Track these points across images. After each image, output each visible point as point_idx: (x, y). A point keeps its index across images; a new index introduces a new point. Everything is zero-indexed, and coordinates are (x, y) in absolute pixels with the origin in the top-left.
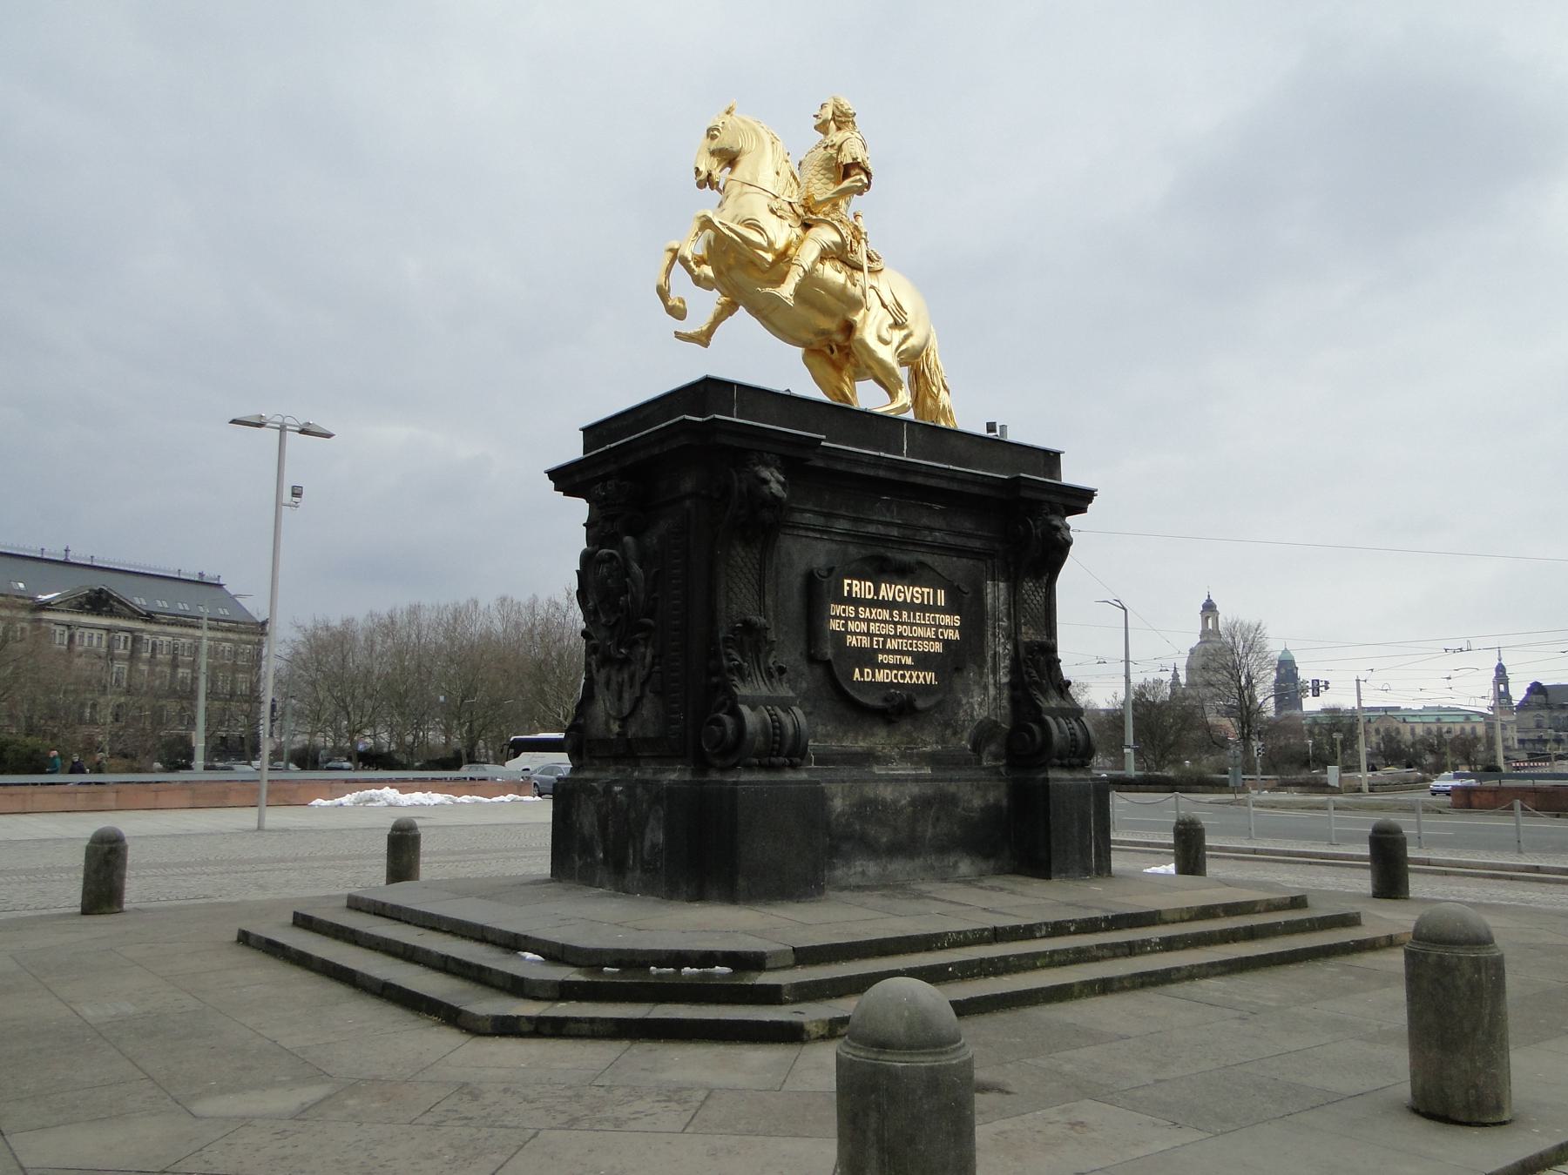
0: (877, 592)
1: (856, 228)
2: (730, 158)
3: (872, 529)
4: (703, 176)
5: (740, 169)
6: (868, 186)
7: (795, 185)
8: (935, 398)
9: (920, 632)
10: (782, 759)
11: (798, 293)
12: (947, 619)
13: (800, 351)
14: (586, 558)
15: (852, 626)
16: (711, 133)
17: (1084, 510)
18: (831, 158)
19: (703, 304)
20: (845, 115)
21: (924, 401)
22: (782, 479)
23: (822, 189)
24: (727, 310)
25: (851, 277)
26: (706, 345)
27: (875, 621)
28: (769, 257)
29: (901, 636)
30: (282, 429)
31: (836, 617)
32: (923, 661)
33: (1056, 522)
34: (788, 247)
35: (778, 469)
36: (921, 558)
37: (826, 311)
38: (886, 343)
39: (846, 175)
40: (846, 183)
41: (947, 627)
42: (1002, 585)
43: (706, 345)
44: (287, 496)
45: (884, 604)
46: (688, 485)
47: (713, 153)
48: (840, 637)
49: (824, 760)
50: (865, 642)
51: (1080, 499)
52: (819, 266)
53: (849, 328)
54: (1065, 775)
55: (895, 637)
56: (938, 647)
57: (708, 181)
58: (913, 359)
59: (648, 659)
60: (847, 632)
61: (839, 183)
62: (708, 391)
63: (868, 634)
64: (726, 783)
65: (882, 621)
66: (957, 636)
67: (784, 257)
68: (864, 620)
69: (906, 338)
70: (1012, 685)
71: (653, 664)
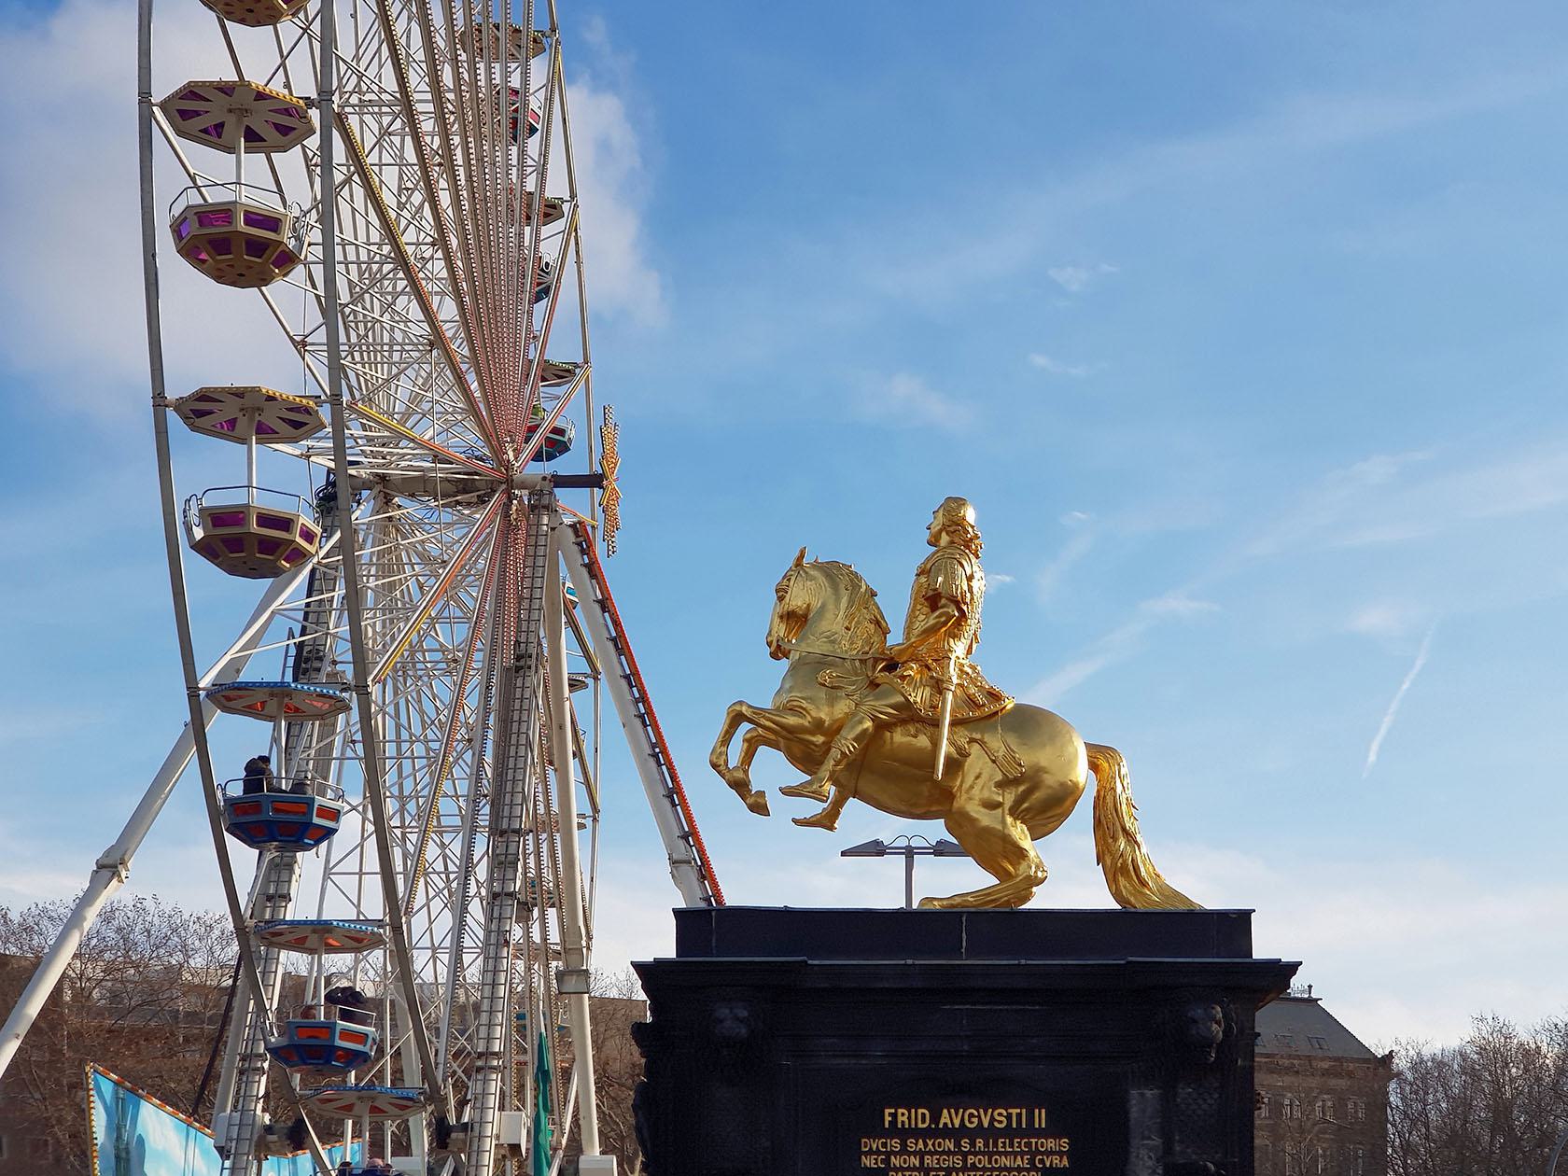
0: (936, 1117)
9: (1005, 1161)
12: (1050, 1144)
27: (931, 1153)
41: (1050, 1153)
42: (1148, 1093)
45: (947, 1132)
65: (943, 1153)
66: (1065, 1162)
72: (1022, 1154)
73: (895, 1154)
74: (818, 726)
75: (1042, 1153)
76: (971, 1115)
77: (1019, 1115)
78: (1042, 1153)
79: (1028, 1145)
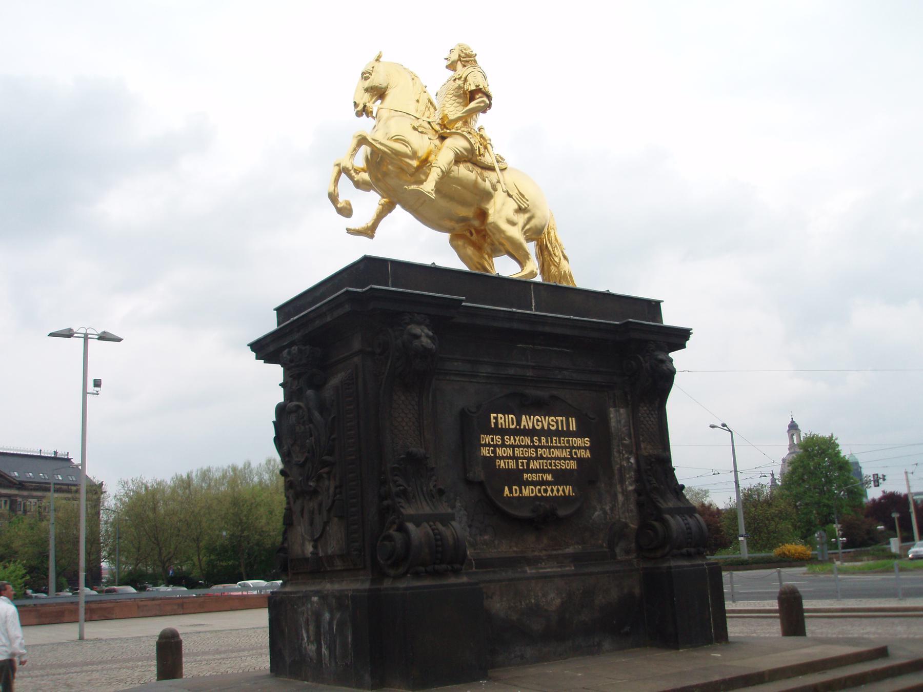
0: (519, 423)
1: (481, 136)
2: (379, 93)
3: (512, 371)
4: (360, 107)
5: (388, 99)
6: (489, 106)
7: (432, 109)
8: (558, 266)
9: (557, 453)
10: (444, 566)
11: (438, 189)
12: (578, 442)
13: (446, 236)
14: (281, 410)
15: (500, 452)
16: (365, 75)
17: (684, 347)
18: (459, 88)
19: (367, 204)
20: (468, 56)
21: (549, 271)
22: (431, 333)
23: (454, 111)
24: (386, 209)
25: (481, 175)
26: (372, 237)
27: (519, 446)
28: (415, 163)
29: (542, 458)
30: (86, 338)
31: (485, 445)
32: (561, 477)
33: (661, 356)
34: (429, 154)
35: (427, 326)
36: (555, 393)
37: (464, 203)
38: (513, 224)
39: (472, 99)
40: (473, 105)
41: (579, 448)
42: (622, 411)
43: (372, 237)
44: (91, 387)
46: (357, 345)
47: (367, 90)
48: (490, 462)
49: (483, 564)
50: (512, 464)
51: (679, 337)
52: (455, 168)
53: (483, 215)
54: (686, 563)
55: (537, 458)
56: (573, 465)
57: (364, 111)
58: (537, 234)
59: (332, 490)
60: (496, 457)
61: (467, 105)
62: (369, 267)
63: (514, 458)
64: (398, 589)
65: (524, 447)
66: (588, 454)
67: (425, 163)
68: (509, 446)
69: (529, 219)
70: (638, 492)
71: (335, 495)
72: (566, 447)
73: (499, 446)
74: (414, 155)
75: (575, 448)
76: (538, 420)
77: (562, 421)
78: (575, 448)
79: (568, 441)
